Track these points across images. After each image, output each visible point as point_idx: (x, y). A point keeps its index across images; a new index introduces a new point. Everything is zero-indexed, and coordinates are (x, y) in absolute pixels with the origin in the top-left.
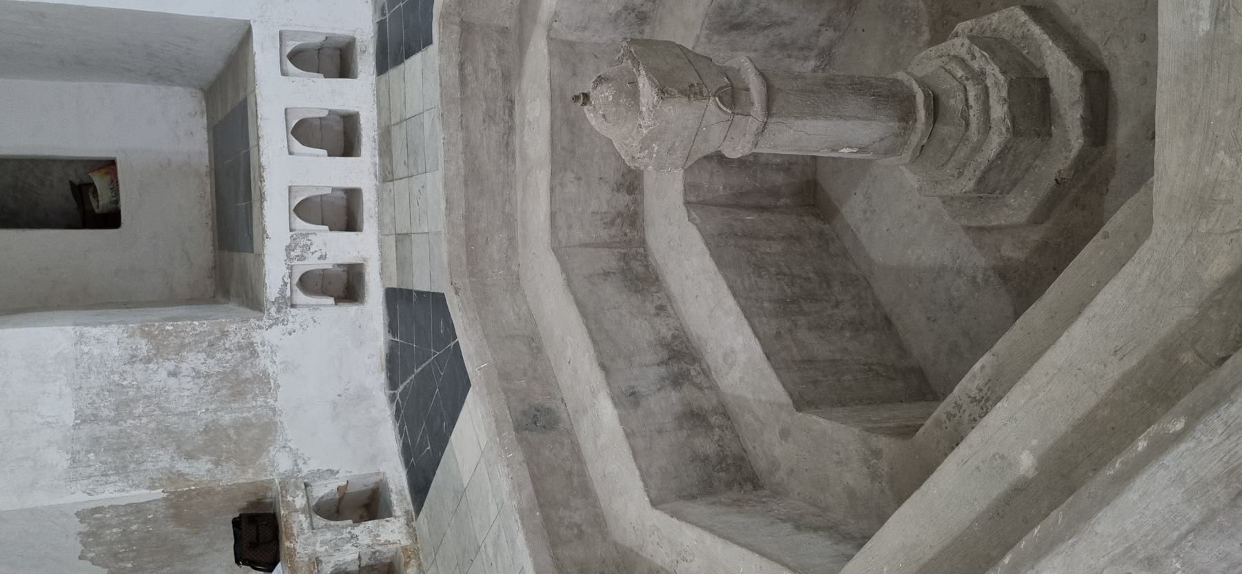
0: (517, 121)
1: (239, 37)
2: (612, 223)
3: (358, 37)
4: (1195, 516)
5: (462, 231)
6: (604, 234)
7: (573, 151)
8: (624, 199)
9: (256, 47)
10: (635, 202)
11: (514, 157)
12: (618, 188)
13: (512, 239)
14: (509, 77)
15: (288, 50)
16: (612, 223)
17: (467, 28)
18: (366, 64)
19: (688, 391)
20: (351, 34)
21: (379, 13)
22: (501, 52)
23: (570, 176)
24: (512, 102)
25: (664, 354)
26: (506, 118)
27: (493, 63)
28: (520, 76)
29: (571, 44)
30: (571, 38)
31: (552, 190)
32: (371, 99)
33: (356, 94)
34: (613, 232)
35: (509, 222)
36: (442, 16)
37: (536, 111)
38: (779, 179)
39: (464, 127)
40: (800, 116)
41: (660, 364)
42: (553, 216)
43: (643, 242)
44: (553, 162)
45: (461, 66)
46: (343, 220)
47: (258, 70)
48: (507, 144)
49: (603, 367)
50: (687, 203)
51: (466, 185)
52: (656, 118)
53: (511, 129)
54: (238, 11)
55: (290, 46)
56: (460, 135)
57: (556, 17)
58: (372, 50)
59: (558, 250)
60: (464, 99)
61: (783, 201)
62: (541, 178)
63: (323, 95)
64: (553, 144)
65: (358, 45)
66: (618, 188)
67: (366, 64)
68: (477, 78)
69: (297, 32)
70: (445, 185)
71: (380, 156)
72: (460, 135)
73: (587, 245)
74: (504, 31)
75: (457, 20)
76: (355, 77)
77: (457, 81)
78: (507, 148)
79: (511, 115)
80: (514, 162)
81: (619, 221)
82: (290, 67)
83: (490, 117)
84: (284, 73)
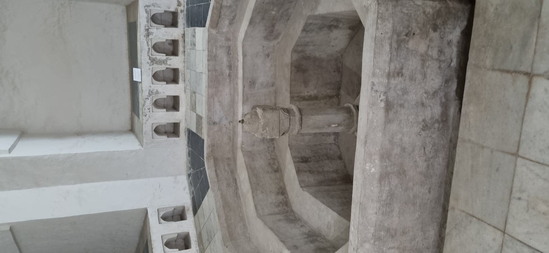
0: (239, 185)
1: (143, 219)
2: (279, 206)
3: (185, 206)
4: (372, 54)
5: (225, 225)
6: (277, 210)
7: (258, 184)
8: (281, 197)
9: (149, 216)
10: (285, 198)
12: (278, 194)
13: (244, 225)
14: (233, 172)
16: (279, 206)
17: (216, 160)
18: (189, 214)
19: (317, 244)
22: (229, 165)
23: (259, 192)
24: (236, 179)
25: (307, 236)
27: (227, 168)
28: (236, 170)
29: (250, 152)
30: (250, 149)
31: (253, 197)
32: (193, 226)
33: (187, 226)
34: (280, 209)
35: (242, 219)
36: (207, 158)
37: (243, 176)
38: (335, 175)
39: (220, 189)
40: (312, 115)
41: (304, 238)
42: (256, 206)
43: (292, 211)
44: (252, 188)
45: (216, 171)
46: (183, 244)
47: (151, 224)
48: (237, 193)
49: (282, 241)
50: (301, 187)
51: (224, 208)
52: (264, 118)
53: (237, 188)
55: (161, 214)
56: (219, 192)
57: (243, 143)
58: (191, 209)
59: (259, 216)
61: (338, 182)
62: (250, 196)
63: (175, 228)
64: (250, 182)
65: (186, 208)
66: (278, 194)
67: (189, 214)
69: (163, 208)
70: (217, 211)
71: (199, 246)
73: (271, 214)
74: (229, 159)
75: (212, 157)
76: (186, 219)
77: (215, 176)
78: (237, 194)
79: (236, 183)
81: (281, 205)
82: (162, 221)
83: (228, 185)
84: (160, 223)
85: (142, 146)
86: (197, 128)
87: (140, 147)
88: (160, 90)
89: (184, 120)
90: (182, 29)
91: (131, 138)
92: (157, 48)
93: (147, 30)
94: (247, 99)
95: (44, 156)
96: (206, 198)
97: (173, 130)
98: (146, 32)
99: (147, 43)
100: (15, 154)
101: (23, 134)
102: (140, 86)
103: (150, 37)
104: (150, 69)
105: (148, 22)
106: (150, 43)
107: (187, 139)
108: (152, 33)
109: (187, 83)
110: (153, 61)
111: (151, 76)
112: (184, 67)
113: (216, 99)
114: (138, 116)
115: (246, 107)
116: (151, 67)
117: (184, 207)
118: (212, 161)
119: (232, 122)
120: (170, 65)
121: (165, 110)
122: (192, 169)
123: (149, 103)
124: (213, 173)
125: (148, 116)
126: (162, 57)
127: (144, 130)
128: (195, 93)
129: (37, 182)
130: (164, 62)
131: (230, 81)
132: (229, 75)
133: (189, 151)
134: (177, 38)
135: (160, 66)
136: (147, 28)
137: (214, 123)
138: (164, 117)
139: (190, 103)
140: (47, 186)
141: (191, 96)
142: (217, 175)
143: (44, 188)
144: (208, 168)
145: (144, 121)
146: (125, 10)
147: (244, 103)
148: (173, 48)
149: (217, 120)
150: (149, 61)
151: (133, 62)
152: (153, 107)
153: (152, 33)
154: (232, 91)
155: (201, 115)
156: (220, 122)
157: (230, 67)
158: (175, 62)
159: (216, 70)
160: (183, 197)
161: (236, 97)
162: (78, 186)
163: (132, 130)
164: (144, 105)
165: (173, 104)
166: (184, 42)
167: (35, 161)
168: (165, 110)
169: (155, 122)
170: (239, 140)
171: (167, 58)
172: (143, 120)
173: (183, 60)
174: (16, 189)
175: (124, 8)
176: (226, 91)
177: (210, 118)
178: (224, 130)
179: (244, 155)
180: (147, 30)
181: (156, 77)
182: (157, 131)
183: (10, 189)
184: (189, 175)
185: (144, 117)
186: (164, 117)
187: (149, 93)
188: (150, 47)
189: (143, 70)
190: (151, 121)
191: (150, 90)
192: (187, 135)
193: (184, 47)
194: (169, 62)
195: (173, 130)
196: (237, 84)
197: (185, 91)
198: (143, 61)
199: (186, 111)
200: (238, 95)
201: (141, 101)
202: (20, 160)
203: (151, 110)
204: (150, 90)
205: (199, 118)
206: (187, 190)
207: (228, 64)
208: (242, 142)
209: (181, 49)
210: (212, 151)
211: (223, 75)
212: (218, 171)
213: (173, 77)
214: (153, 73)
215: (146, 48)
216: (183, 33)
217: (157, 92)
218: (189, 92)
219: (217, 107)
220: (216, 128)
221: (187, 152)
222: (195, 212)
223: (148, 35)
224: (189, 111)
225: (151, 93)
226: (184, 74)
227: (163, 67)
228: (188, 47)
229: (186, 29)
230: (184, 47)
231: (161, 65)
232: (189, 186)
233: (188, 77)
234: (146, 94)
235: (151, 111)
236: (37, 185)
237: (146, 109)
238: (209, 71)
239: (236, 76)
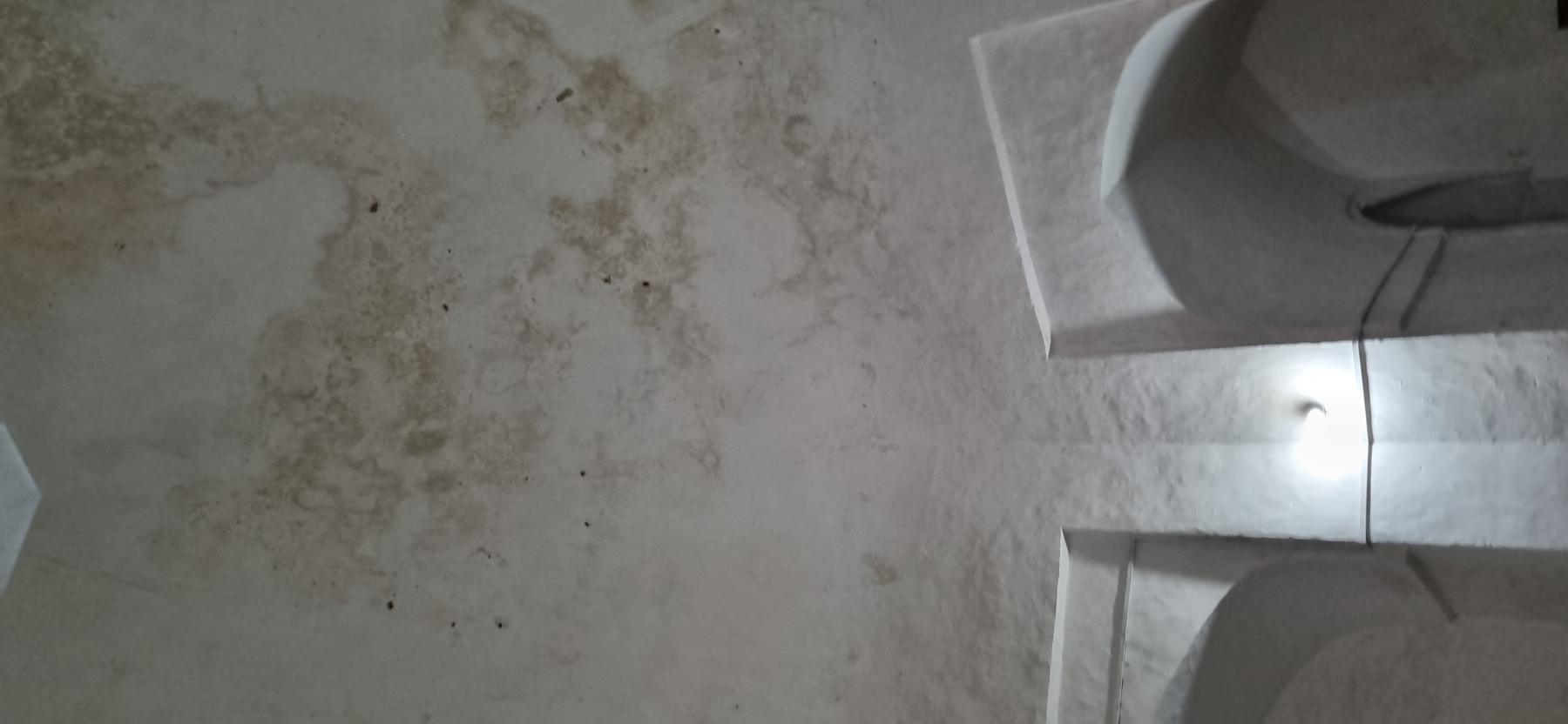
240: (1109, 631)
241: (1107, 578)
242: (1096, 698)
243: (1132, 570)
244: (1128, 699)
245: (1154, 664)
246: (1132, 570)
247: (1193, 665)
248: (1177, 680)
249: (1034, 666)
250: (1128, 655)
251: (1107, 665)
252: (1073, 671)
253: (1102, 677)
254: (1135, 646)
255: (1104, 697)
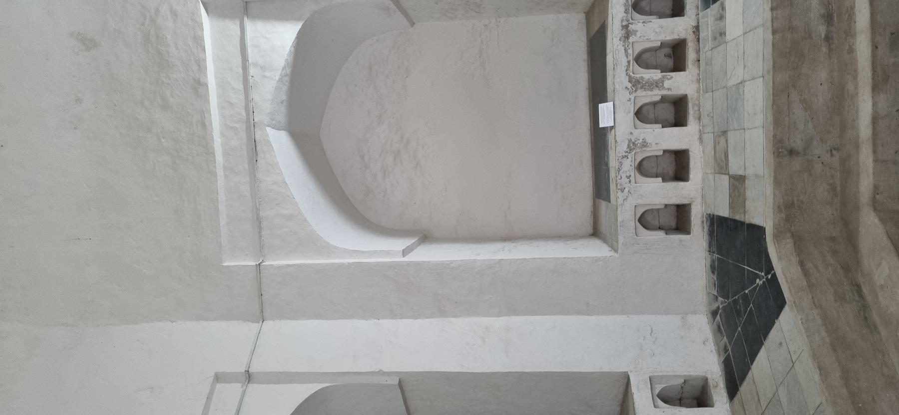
0: (869, 299)
1: (621, 396)
3: (709, 376)
5: (844, 391)
9: (634, 389)
11: (876, 327)
15: (657, 391)
18: (719, 395)
20: (703, 374)
21: (722, 353)
22: (834, 252)
26: (857, 298)
27: (830, 259)
45: (802, 263)
47: (637, 405)
48: (866, 318)
53: (864, 308)
54: (619, 367)
57: (876, 189)
58: (722, 385)
60: (811, 286)
65: (711, 383)
68: (818, 271)
69: (662, 377)
72: (816, 312)
74: (832, 239)
75: (789, 235)
76: (711, 406)
80: (879, 333)
82: (660, 403)
84: (655, 407)
85: (616, 251)
86: (732, 206)
87: (612, 253)
88: (649, 140)
89: (699, 200)
90: (694, 17)
91: (596, 243)
92: (641, 60)
93: (626, 27)
94: (886, 79)
95: (452, 262)
96: (762, 355)
97: (678, 219)
98: (624, 32)
99: (626, 50)
100: (411, 257)
101: (425, 237)
102: (611, 137)
103: (631, 40)
104: (629, 100)
105: (626, 12)
106: (630, 51)
107: (706, 236)
108: (635, 32)
109: (706, 120)
110: (636, 84)
111: (632, 114)
112: (698, 91)
113: (795, 96)
114: (608, 199)
115: (882, 98)
116: (632, 97)
117: (706, 380)
118: (789, 244)
119: (837, 149)
120: (669, 89)
121: (660, 179)
122: (720, 299)
123: (628, 166)
124: (796, 270)
125: (626, 190)
126: (656, 75)
127: (620, 219)
128: (725, 133)
129: (441, 308)
130: (658, 84)
131: (830, 50)
132: (828, 38)
133: (713, 261)
134: (682, 36)
135: (650, 93)
136: (624, 24)
137: (792, 152)
138: (659, 193)
139: (712, 161)
140: (455, 316)
141: (716, 143)
142: (806, 273)
143: (453, 319)
144: (780, 258)
145: (620, 201)
146: (584, 21)
147: (876, 88)
148: (675, 56)
149: (798, 145)
150: (629, 85)
151: (598, 92)
152: (637, 174)
153: (635, 32)
154: (836, 74)
155: (741, 173)
156: (805, 149)
157: (828, 18)
158: (680, 83)
159: (792, 28)
160: (704, 360)
161: (850, 86)
162: (503, 321)
163: (596, 233)
164: (619, 170)
165: (678, 166)
166: (698, 41)
167: (438, 270)
168: (660, 179)
169: (640, 202)
170: (866, 184)
171: (663, 77)
172: (617, 198)
173: (695, 77)
174: (411, 318)
175: (582, 16)
176: (819, 77)
177: (781, 141)
178: (818, 168)
179: (882, 220)
180: (626, 27)
181: (640, 115)
182: (645, 221)
183: (402, 317)
184: (714, 314)
185: (620, 194)
186: (659, 193)
187: (629, 146)
188: (631, 58)
189: (617, 103)
190: (632, 201)
191: (630, 141)
192: (706, 229)
193: (698, 51)
194: (667, 84)
195: (678, 219)
196: (851, 50)
197: (701, 139)
198: (617, 86)
199: (703, 180)
200: (855, 78)
201: (613, 163)
202: (417, 265)
203: (632, 178)
204: (630, 141)
205: (738, 182)
206: (711, 345)
207: (823, 11)
208: (876, 187)
209: (691, 55)
210: (788, 219)
211: (810, 37)
212: (809, 265)
213: (677, 112)
214: (637, 107)
215: (623, 60)
216: (694, 24)
217: (645, 144)
218: (709, 138)
219: (798, 111)
220: (797, 164)
221: (709, 263)
222: (733, 390)
223: (627, 34)
224: (711, 177)
225: (632, 146)
226: (699, 106)
227: (655, 95)
228: (707, 45)
229: (701, 14)
230: (698, 51)
231: (652, 90)
232: (714, 335)
233: (707, 106)
234: (623, 147)
235: (633, 181)
236: (442, 313)
237: (624, 176)
238: (774, 32)
239: (850, 33)
240: (240, 59)
241: (233, 27)
242: (238, 98)
243: (245, 18)
244: (255, 95)
245: (267, 74)
246: (245, 18)
247: (288, 71)
248: (281, 80)
249: (199, 86)
250: (252, 71)
251: (241, 78)
252: (222, 86)
253: (240, 86)
254: (255, 65)
255: (242, 97)
